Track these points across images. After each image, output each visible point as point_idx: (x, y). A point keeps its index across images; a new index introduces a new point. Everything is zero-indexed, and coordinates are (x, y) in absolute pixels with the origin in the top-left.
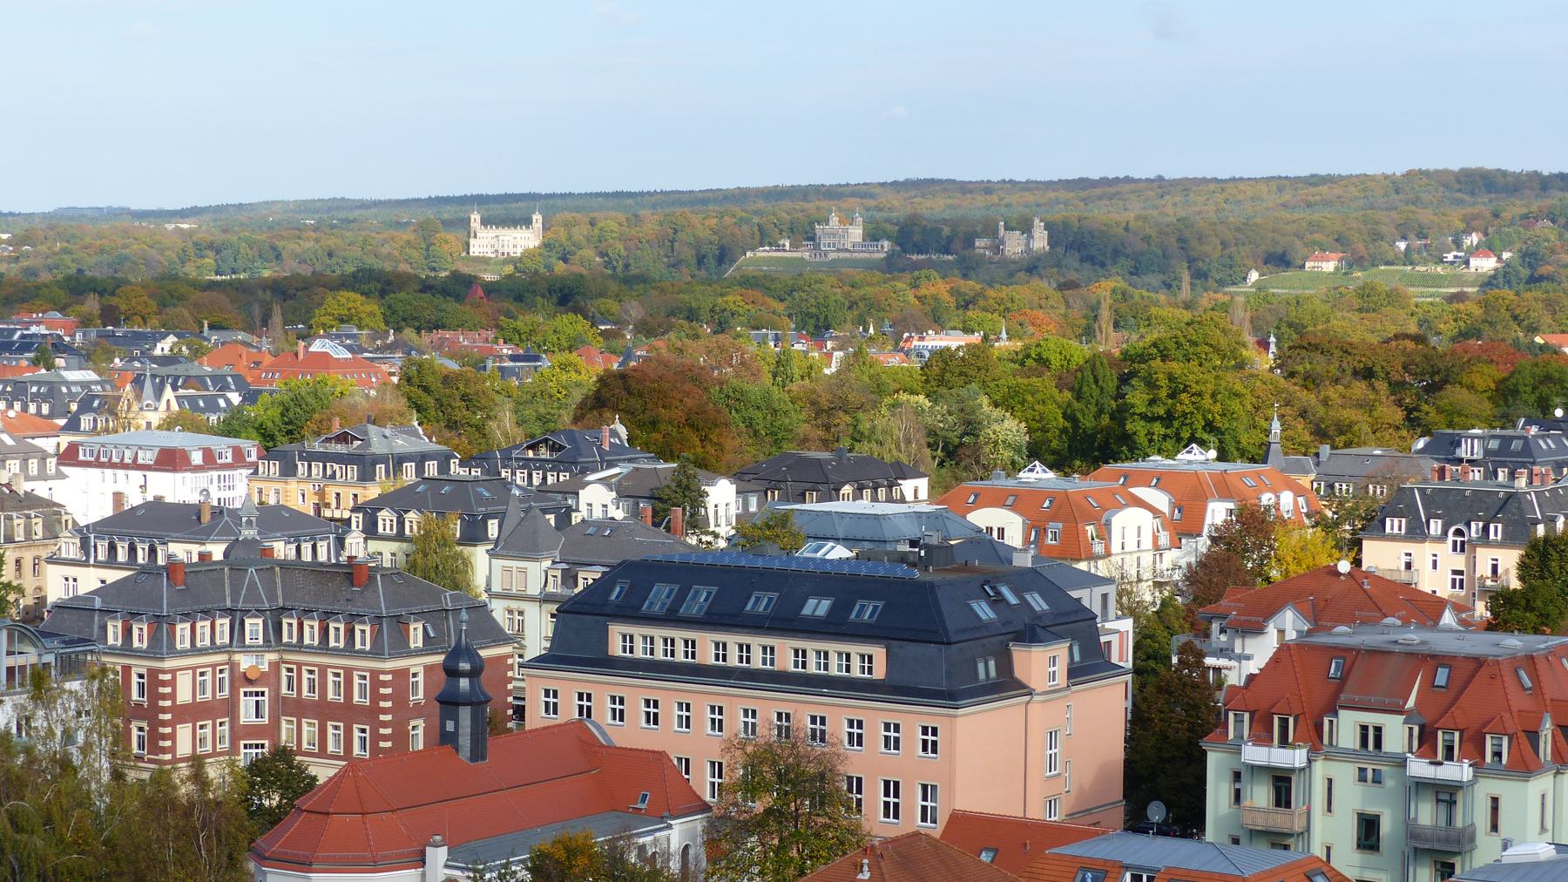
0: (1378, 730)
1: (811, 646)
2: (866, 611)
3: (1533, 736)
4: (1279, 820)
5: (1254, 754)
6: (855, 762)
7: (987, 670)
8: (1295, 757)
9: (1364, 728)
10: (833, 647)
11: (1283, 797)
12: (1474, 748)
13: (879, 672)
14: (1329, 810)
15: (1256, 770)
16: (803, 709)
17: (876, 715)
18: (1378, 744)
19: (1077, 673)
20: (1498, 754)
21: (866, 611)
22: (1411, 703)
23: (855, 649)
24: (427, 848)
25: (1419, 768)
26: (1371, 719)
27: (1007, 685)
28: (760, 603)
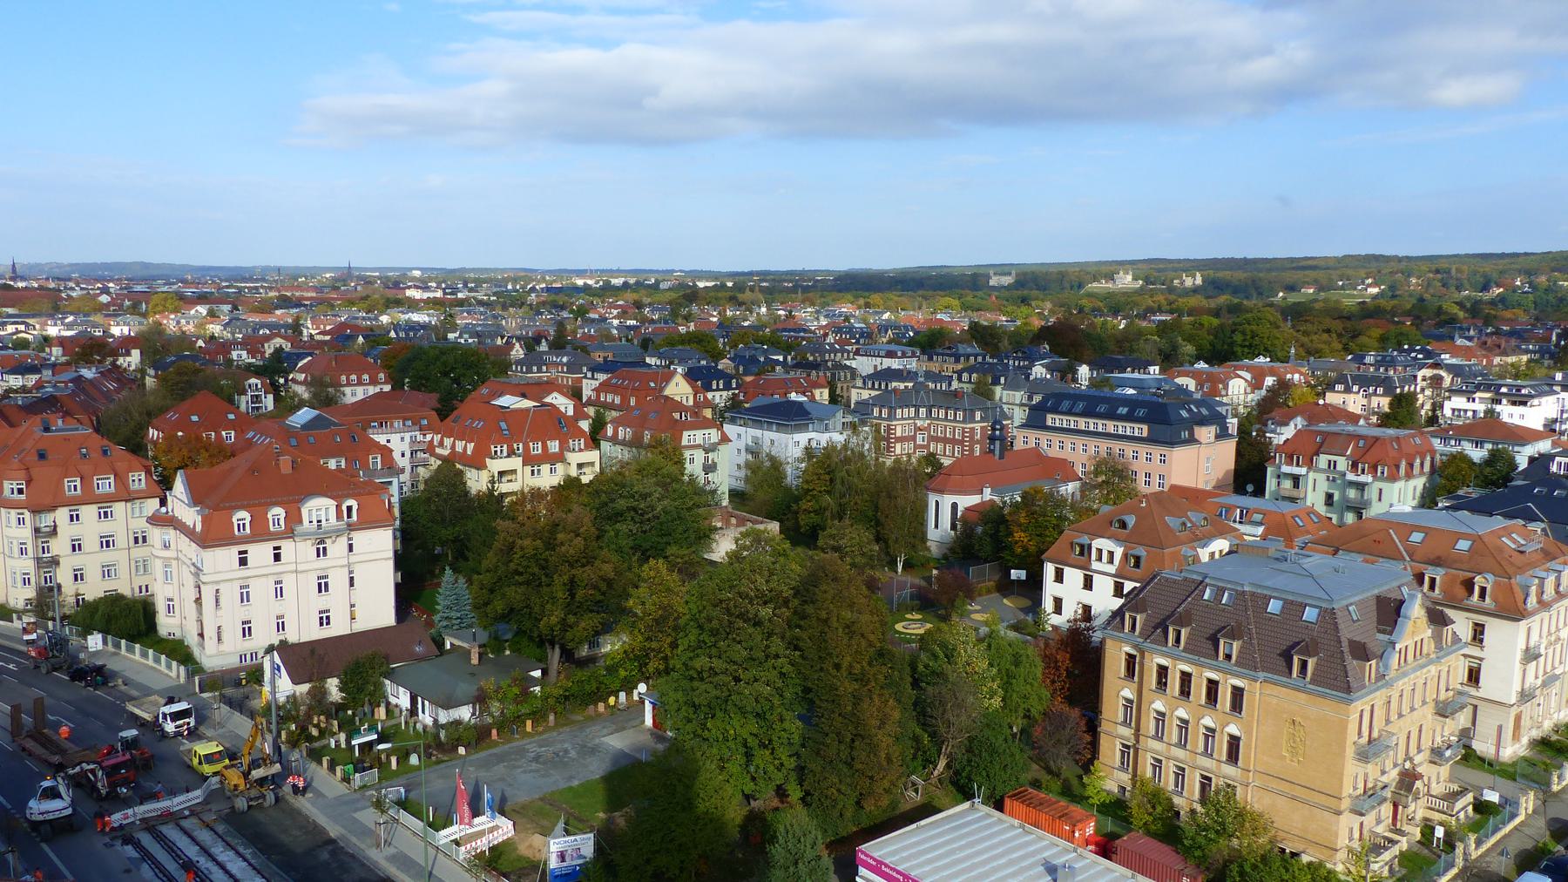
0: (1335, 462)
1: (1120, 424)
2: (1141, 412)
3: (1398, 467)
4: (1295, 493)
5: (1286, 469)
6: (1135, 466)
7: (1185, 435)
8: (1303, 471)
9: (1330, 461)
10: (1128, 425)
11: (1296, 485)
12: (1374, 469)
13: (1145, 434)
14: (1380, 500)
15: (1287, 475)
16: (1117, 446)
17: (1143, 449)
18: (1335, 467)
19: (1218, 437)
20: (1383, 473)
21: (1141, 412)
22: (1348, 453)
23: (1136, 426)
24: (1423, 535)
25: (1351, 477)
26: (1333, 458)
27: (1192, 440)
28: (1102, 408)
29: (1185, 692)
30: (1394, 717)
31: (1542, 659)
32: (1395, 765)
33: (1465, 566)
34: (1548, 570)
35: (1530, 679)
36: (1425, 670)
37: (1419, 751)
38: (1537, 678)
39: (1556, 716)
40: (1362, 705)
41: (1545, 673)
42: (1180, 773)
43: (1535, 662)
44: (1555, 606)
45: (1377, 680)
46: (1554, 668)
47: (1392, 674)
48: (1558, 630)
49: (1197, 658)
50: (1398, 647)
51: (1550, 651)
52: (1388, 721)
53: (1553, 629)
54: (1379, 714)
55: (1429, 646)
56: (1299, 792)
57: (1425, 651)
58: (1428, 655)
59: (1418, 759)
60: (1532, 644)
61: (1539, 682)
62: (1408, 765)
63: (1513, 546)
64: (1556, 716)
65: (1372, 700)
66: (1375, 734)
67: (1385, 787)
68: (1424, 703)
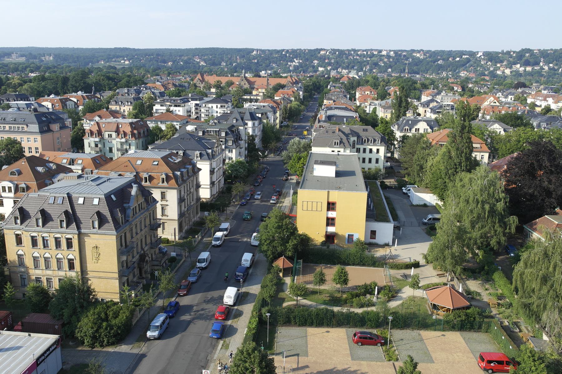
0: (111, 135)
9: (109, 134)
29: (45, 246)
30: (134, 235)
31: (186, 200)
32: (138, 253)
33: (156, 171)
34: (185, 168)
35: (183, 208)
36: (144, 214)
37: (146, 245)
38: (185, 207)
39: (193, 220)
40: (121, 233)
41: (188, 205)
42: (49, 280)
43: (184, 203)
44: (188, 181)
45: (125, 223)
46: (190, 203)
47: (131, 219)
48: (190, 189)
49: (49, 230)
50: (132, 208)
51: (189, 197)
52: (132, 237)
53: (188, 189)
54: (128, 235)
55: (144, 205)
56: (102, 275)
57: (143, 207)
58: (144, 208)
59: (146, 249)
60: (182, 196)
61: (186, 209)
62: (142, 252)
63: (172, 161)
64: (193, 220)
65: (124, 231)
66: (128, 243)
67: (134, 263)
68: (145, 226)
